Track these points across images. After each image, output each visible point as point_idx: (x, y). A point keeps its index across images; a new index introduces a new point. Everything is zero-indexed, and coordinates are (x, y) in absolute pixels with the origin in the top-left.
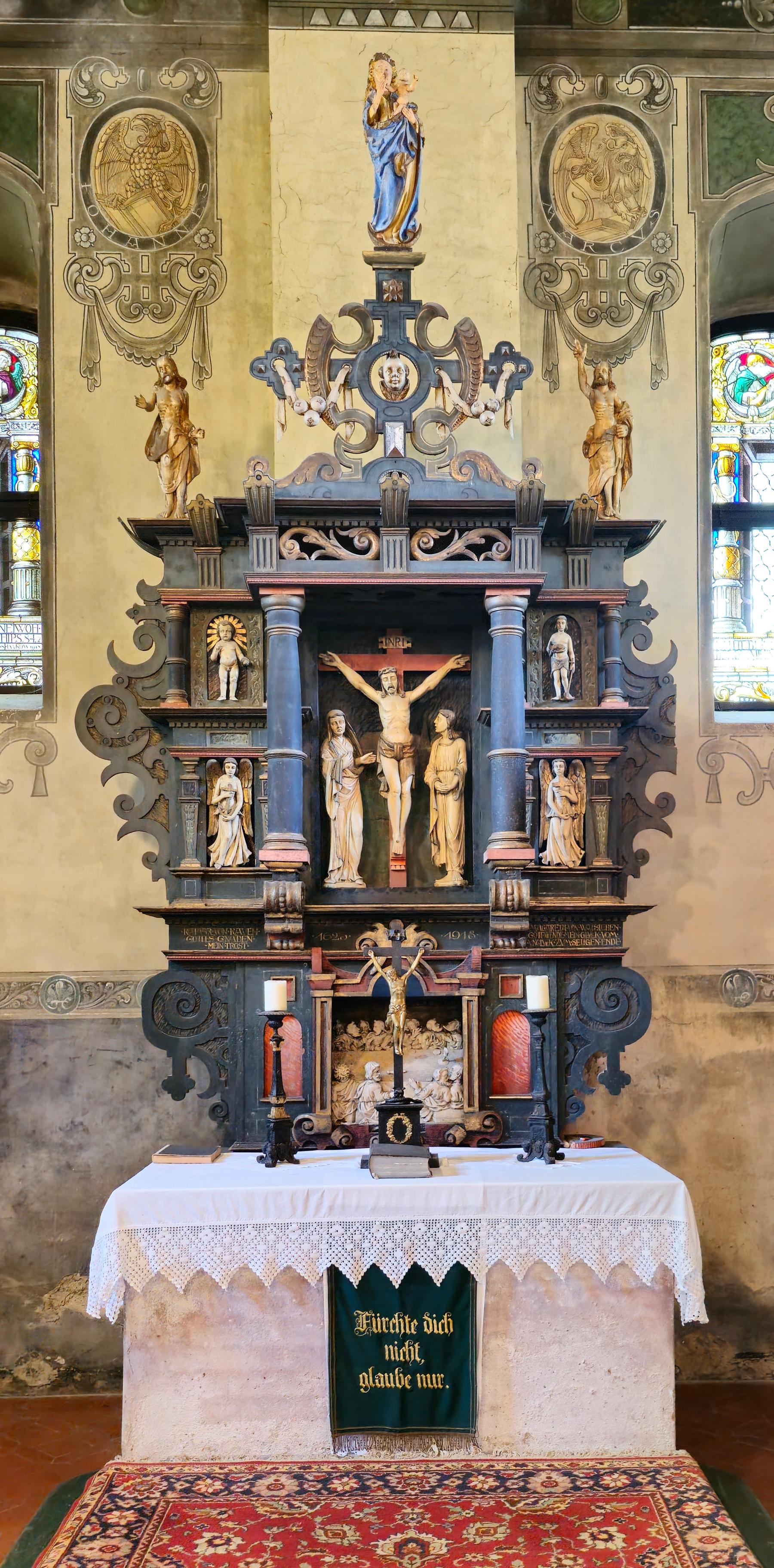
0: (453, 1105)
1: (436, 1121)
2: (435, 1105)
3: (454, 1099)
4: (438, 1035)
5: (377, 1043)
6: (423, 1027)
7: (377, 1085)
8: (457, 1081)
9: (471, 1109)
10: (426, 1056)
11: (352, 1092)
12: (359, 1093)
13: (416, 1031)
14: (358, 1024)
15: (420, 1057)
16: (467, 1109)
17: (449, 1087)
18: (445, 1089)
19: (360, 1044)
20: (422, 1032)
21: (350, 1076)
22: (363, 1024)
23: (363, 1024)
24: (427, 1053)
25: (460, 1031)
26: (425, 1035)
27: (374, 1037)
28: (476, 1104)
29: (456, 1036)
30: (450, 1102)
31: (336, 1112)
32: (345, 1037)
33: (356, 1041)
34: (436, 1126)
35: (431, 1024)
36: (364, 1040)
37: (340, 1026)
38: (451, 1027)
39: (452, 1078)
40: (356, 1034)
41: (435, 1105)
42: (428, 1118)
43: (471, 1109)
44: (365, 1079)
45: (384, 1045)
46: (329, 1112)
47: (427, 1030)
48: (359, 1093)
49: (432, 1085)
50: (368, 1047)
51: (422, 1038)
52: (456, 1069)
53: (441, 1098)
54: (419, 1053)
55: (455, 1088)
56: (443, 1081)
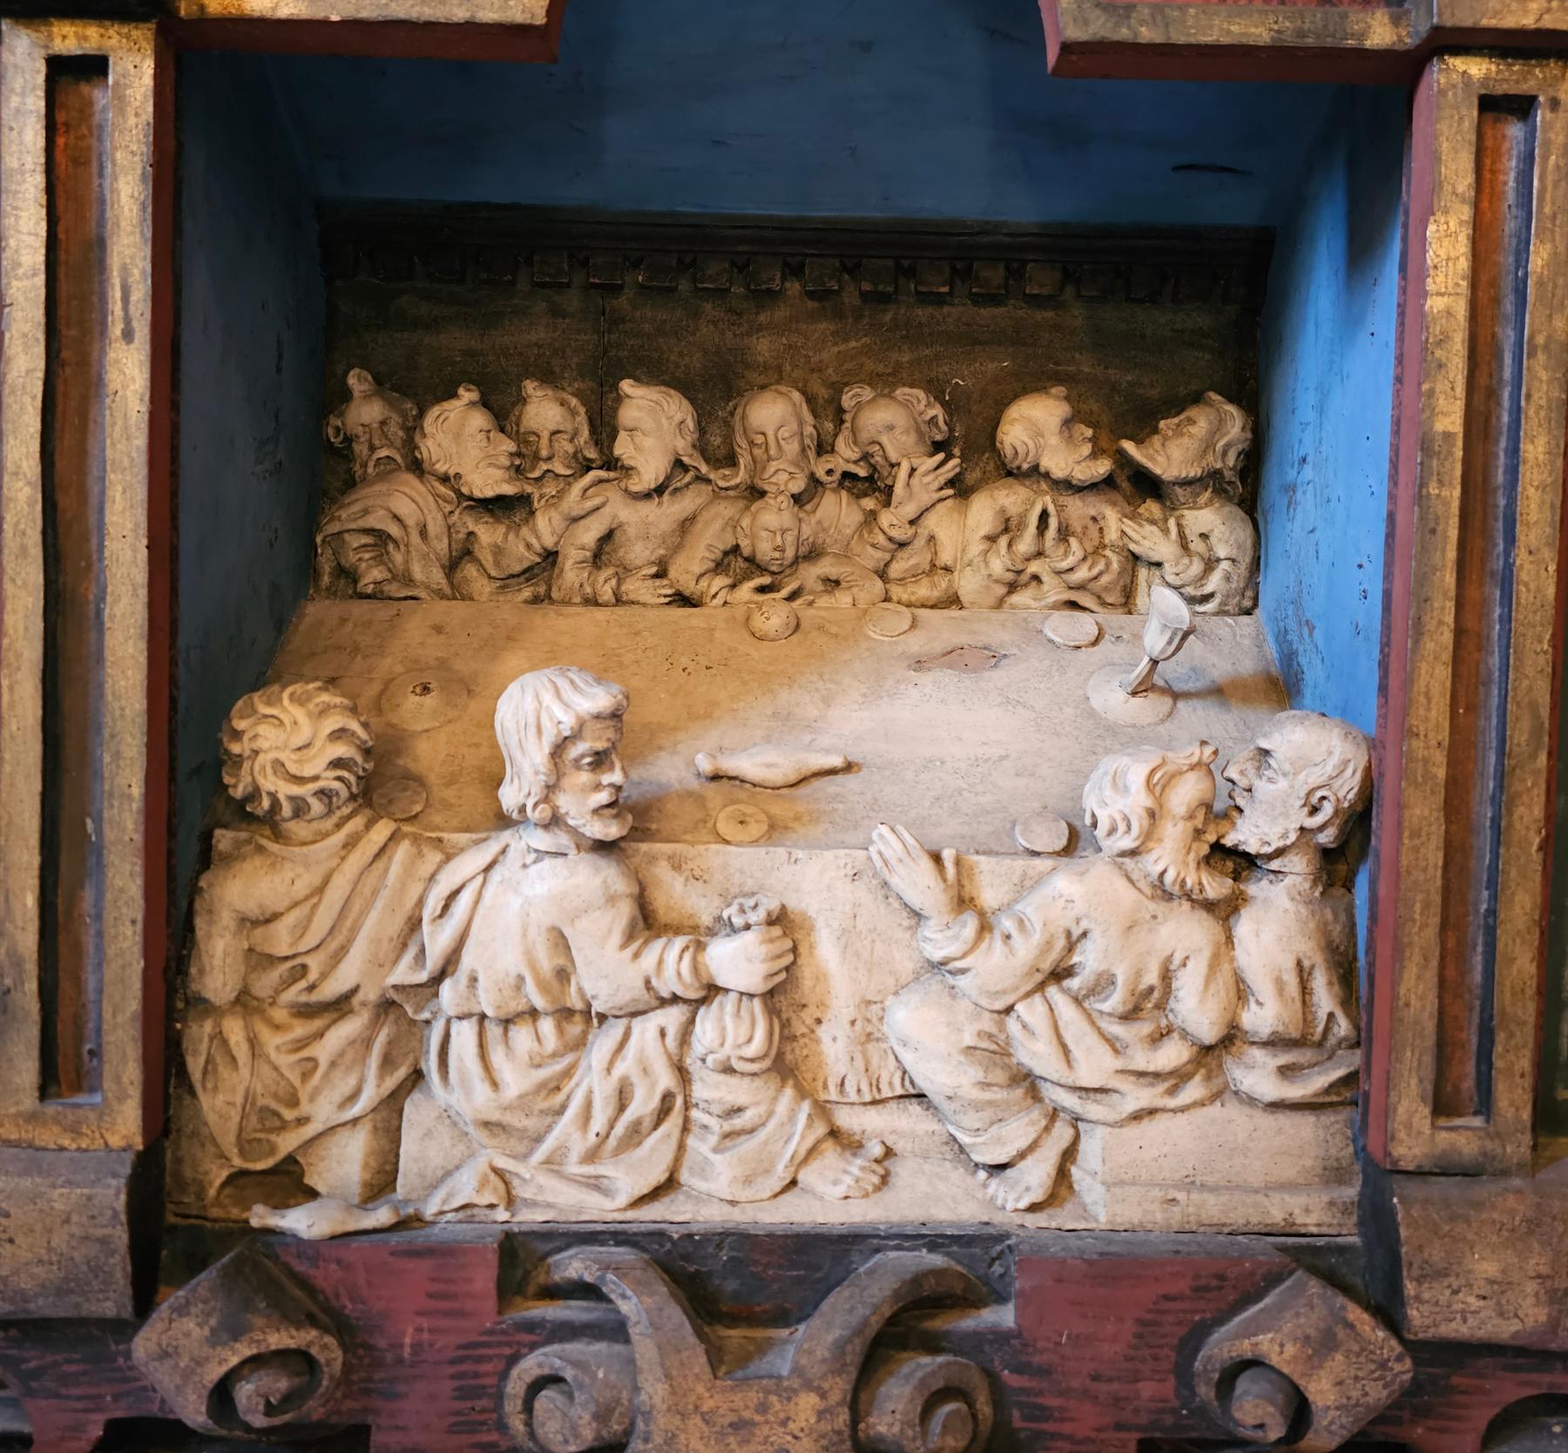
0: (1257, 1075)
1: (1101, 1205)
2: (1094, 1065)
3: (1262, 1017)
4: (1078, 509)
5: (639, 553)
6: (973, 455)
7: (593, 879)
8: (1298, 866)
9: (1463, 1138)
10: (994, 657)
11: (378, 924)
12: (437, 941)
13: (920, 479)
14: (502, 410)
15: (952, 657)
16: (1414, 1134)
17: (1225, 911)
18: (1187, 934)
19: (520, 553)
20: (960, 488)
21: (379, 782)
22: (545, 411)
23: (545, 411)
24: (995, 630)
25: (1246, 485)
26: (983, 510)
27: (619, 510)
28: (1514, 1099)
29: (1211, 521)
30: (1232, 1037)
31: (219, 1106)
32: (404, 503)
33: (488, 534)
34: (1113, 1268)
35: (1036, 425)
36: (546, 527)
37: (366, 411)
38: (1172, 453)
39: (1247, 835)
40: (488, 481)
41: (1094, 1065)
42: (1036, 1176)
43: (1463, 1138)
44: (503, 821)
45: (688, 570)
46: (125, 1124)
47: (1009, 473)
48: (437, 941)
49: (1069, 893)
50: (571, 574)
51: (965, 531)
52: (1304, 765)
53: (1149, 1004)
54: (942, 629)
55: (1277, 928)
56: (1170, 856)
